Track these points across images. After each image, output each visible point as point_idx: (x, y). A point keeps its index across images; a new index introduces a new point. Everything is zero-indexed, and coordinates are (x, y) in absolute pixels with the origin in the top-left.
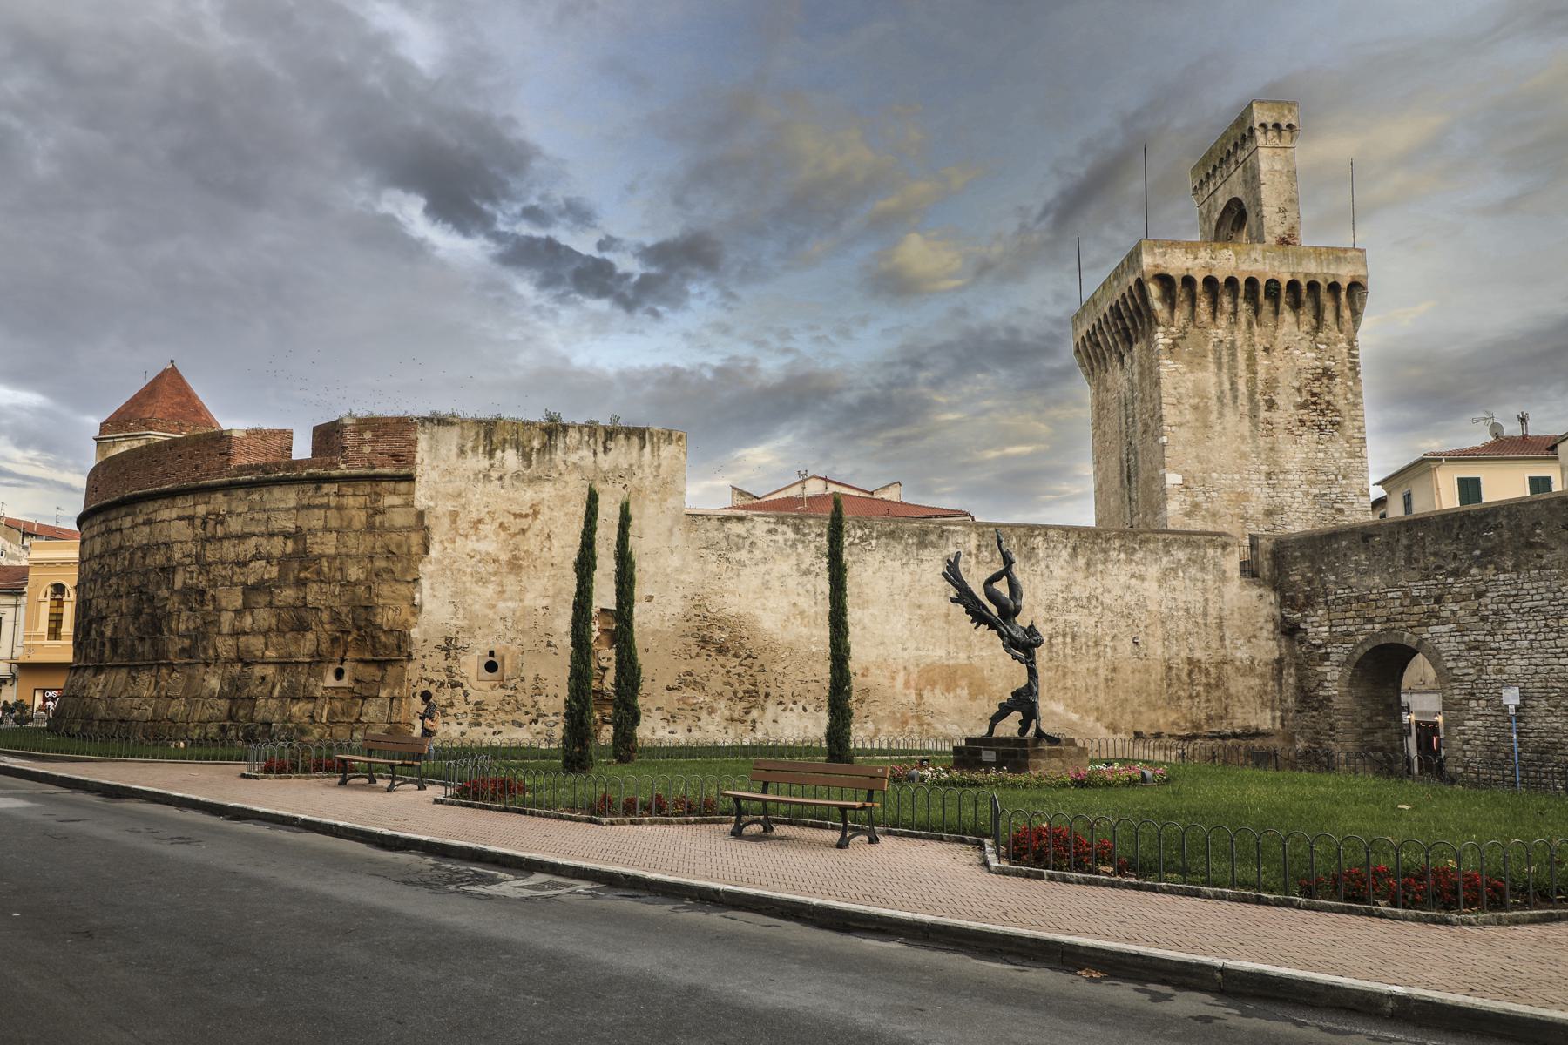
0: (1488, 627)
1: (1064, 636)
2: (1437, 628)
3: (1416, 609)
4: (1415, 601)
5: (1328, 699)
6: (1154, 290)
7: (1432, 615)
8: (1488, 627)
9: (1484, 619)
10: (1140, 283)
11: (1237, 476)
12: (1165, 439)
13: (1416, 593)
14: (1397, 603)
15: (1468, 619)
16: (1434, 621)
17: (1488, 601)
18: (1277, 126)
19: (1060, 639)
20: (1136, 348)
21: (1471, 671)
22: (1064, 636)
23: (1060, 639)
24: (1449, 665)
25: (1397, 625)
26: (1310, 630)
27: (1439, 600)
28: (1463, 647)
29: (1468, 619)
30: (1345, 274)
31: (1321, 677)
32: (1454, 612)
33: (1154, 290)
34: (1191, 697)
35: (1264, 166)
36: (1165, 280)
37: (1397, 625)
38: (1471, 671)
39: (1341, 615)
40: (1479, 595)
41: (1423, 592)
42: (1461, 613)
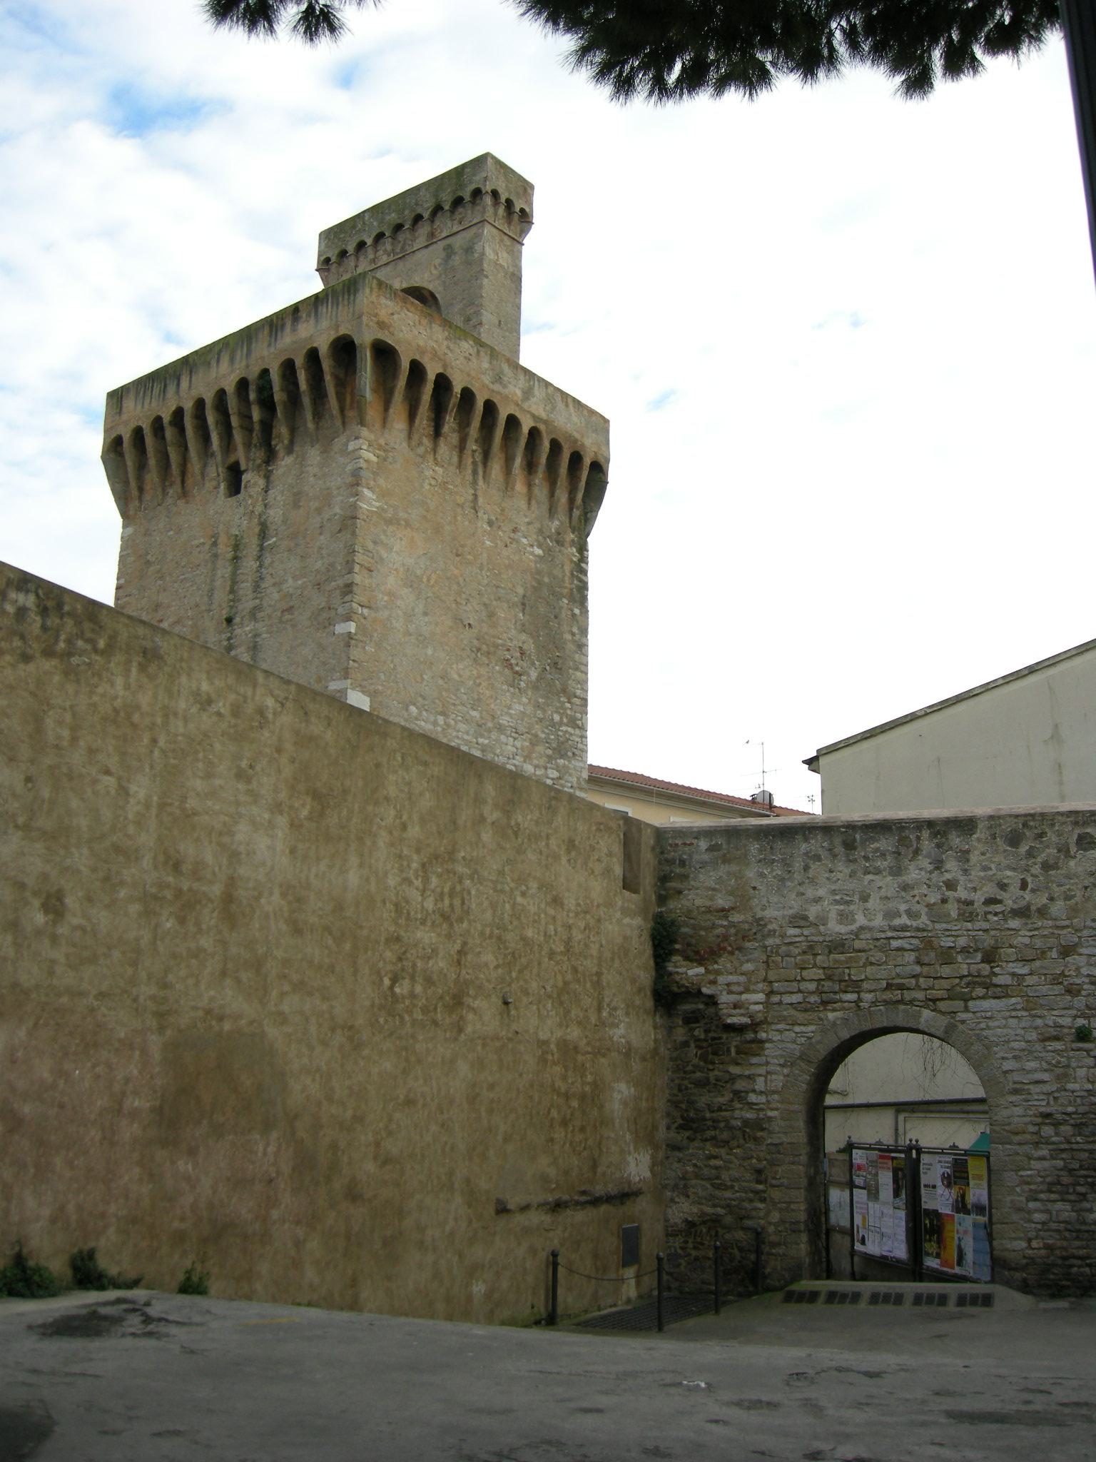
0: (1080, 1002)
1: (413, 978)
2: (986, 1004)
3: (946, 971)
4: (947, 957)
5: (758, 1125)
6: (366, 363)
7: (975, 980)
8: (1080, 1002)
9: (1072, 991)
10: (345, 349)
11: (441, 719)
12: (352, 627)
13: (947, 942)
14: (911, 957)
15: (1044, 989)
16: (980, 991)
17: (1081, 961)
18: (509, 203)
19: (406, 982)
20: (285, 463)
21: (1046, 1076)
22: (413, 978)
23: (406, 982)
24: (1008, 1065)
25: (908, 995)
26: (724, 998)
27: (990, 957)
28: (1033, 1036)
29: (1044, 989)
30: (589, 444)
31: (740, 1085)
32: (1019, 977)
33: (366, 363)
34: (564, 1123)
35: (490, 254)
36: (384, 353)
37: (908, 995)
38: (1046, 1076)
39: (794, 973)
40: (1067, 951)
41: (962, 942)
42: (1030, 980)
